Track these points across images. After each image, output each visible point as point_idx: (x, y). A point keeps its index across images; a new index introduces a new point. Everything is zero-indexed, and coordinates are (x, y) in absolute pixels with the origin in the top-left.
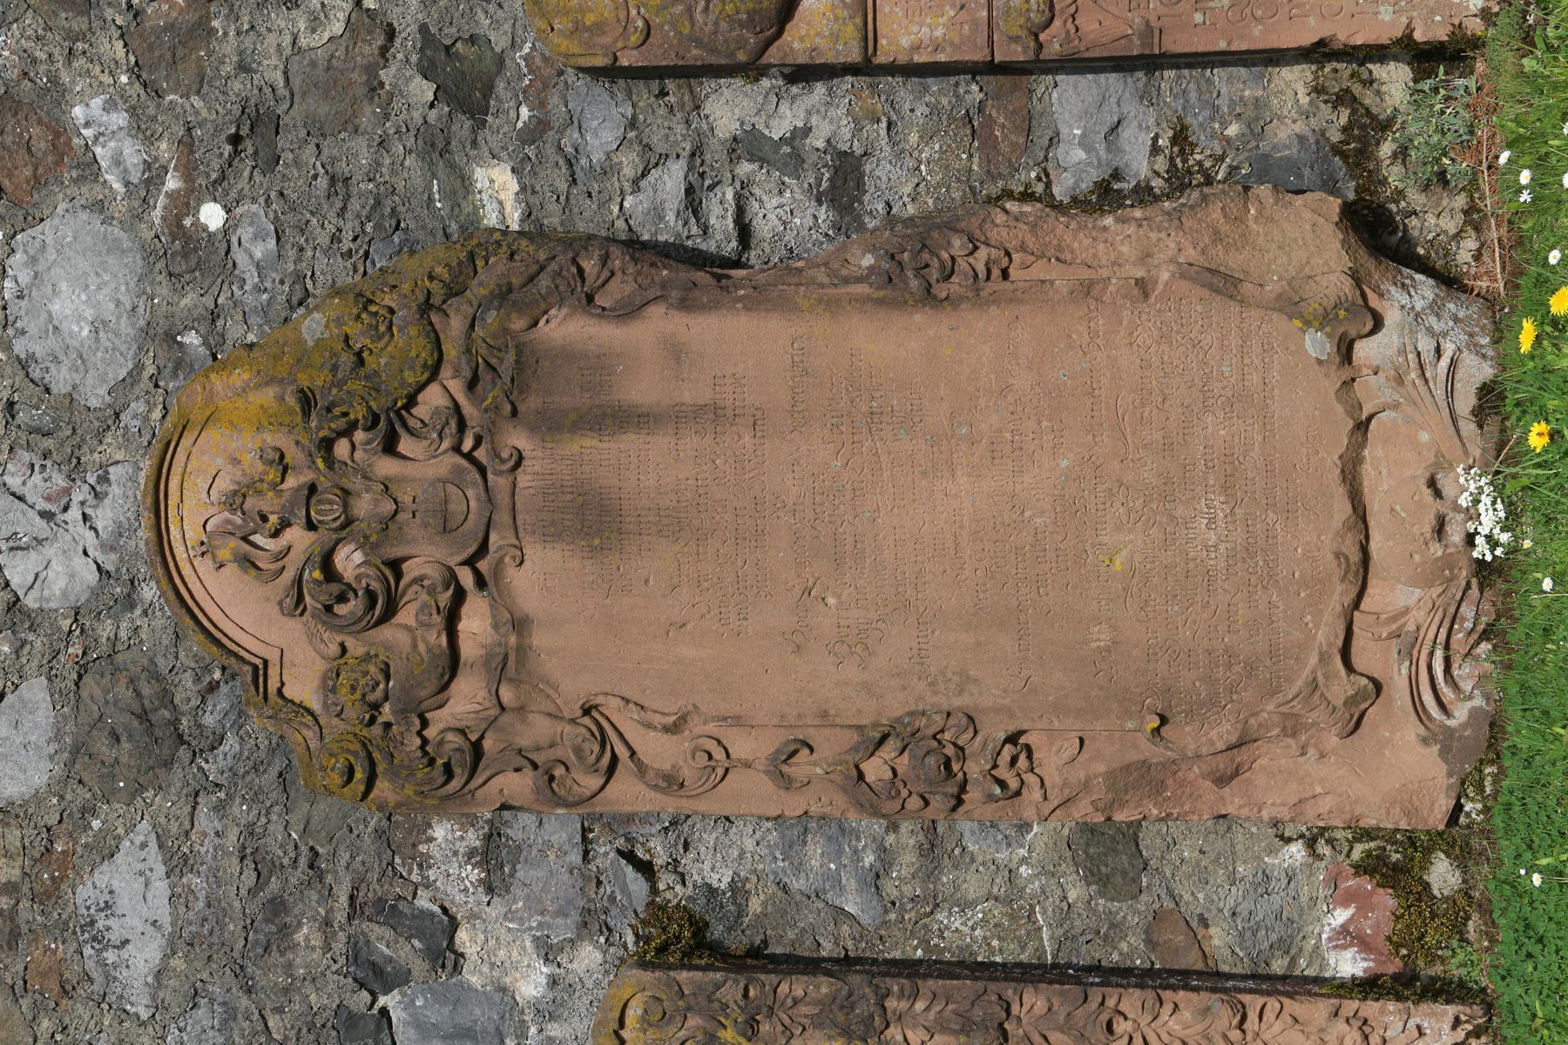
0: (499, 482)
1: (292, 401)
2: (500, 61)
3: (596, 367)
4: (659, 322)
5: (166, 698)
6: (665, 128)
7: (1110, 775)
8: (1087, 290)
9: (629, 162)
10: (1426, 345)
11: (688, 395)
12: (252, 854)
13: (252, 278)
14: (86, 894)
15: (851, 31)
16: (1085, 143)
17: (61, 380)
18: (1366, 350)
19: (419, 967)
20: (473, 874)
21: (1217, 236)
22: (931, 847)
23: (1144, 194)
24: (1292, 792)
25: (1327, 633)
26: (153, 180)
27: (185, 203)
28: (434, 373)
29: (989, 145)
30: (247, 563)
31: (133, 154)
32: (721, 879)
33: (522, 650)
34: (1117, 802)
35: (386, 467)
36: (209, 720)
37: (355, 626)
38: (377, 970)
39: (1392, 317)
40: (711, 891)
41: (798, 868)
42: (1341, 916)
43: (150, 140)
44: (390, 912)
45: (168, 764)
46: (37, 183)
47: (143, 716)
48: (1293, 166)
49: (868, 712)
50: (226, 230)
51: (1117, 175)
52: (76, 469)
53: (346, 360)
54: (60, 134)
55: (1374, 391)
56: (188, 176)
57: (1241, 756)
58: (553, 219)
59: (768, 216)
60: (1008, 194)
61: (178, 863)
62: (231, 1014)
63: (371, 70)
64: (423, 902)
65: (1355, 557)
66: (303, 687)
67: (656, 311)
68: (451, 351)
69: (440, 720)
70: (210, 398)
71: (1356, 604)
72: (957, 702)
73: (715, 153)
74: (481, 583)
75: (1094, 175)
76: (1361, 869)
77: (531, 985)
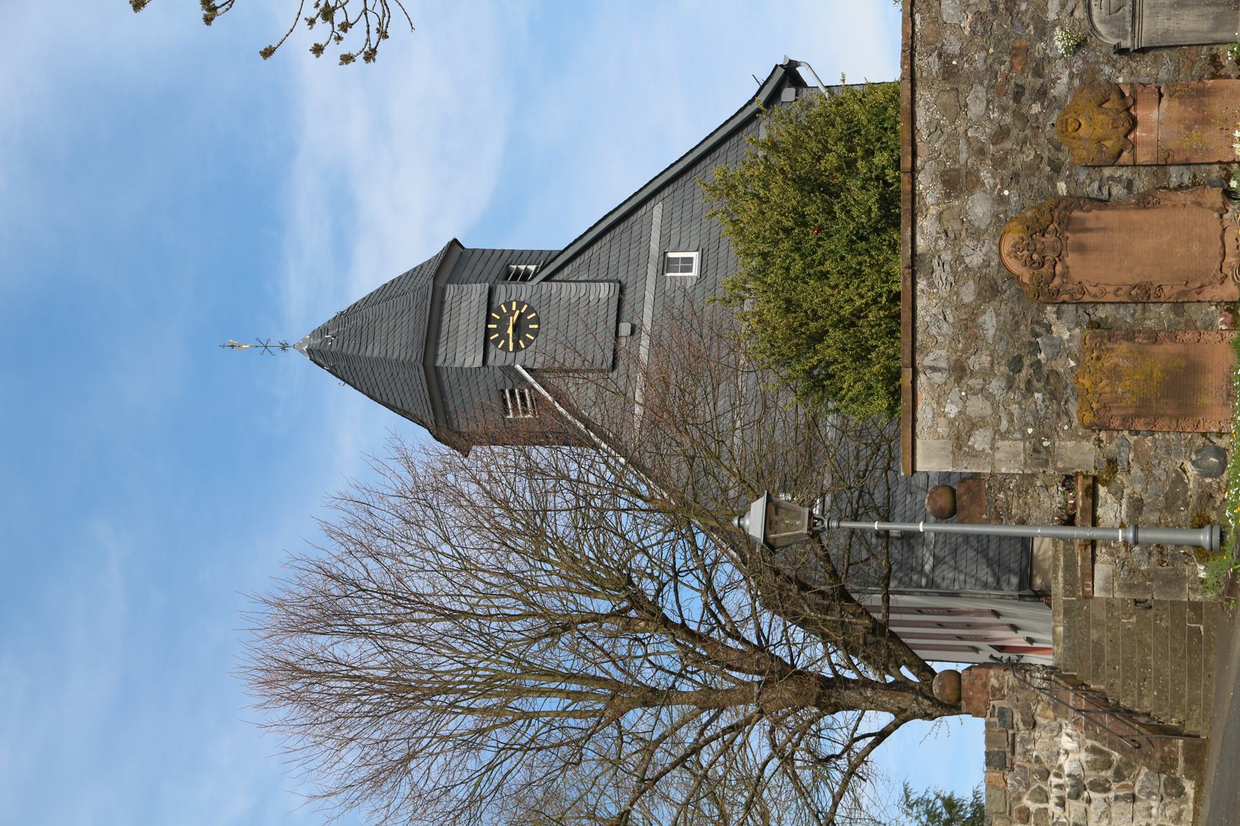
0: (1064, 242)
1: (1025, 227)
2: (1063, 163)
3: (1083, 221)
4: (1095, 212)
5: (996, 283)
6: (1095, 175)
7: (1177, 293)
8: (1174, 206)
9: (1088, 182)
10: (1236, 215)
11: (1099, 226)
12: (1012, 313)
13: (1014, 204)
14: (980, 320)
15: (1131, 159)
16: (1176, 177)
17: (976, 224)
18: (1225, 216)
19: (1044, 333)
20: (1055, 316)
21: (1199, 196)
22: (1144, 310)
23: (1187, 187)
24: (1211, 295)
25: (1217, 266)
26: (996, 187)
27: (1001, 190)
28: (1052, 222)
29: (1158, 178)
30: (1016, 257)
31: (992, 181)
32: (1103, 316)
33: (1068, 272)
34: (1178, 298)
35: (1043, 239)
36: (1004, 288)
37: (1035, 269)
38: (1036, 334)
39: (1230, 210)
40: (1101, 318)
41: (1118, 313)
42: (1222, 319)
43: (995, 179)
44: (1039, 323)
45: (996, 296)
46: (973, 187)
47: (992, 287)
48: (1215, 182)
49: (1132, 282)
50: (1009, 195)
51: (1182, 183)
52: (979, 240)
53: (1035, 220)
54: (978, 178)
55: (1226, 223)
56: (1002, 185)
57: (1202, 289)
58: (1073, 192)
59: (1115, 191)
60: (1161, 187)
61: (998, 315)
62: (1008, 343)
63: (1038, 165)
64: (1045, 321)
65: (1222, 252)
66: (1026, 280)
67: (1094, 211)
68: (1055, 218)
69: (1051, 285)
70: (1009, 228)
71: (1223, 261)
72: (1149, 280)
73: (1105, 180)
74: (1060, 260)
75: (1178, 183)
76: (1225, 310)
77: (1066, 336)
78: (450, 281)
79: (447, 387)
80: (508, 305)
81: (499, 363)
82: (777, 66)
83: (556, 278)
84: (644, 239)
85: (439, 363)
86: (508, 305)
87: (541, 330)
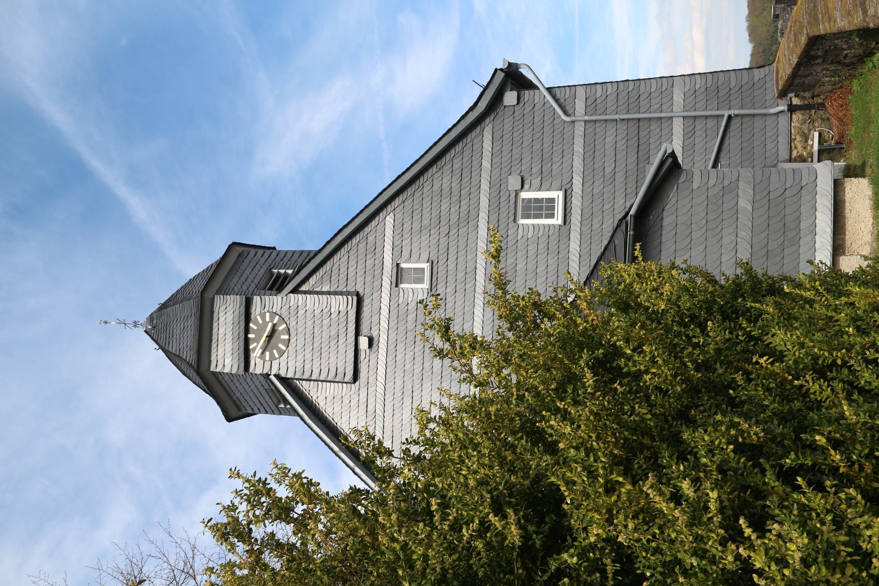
78: (219, 292)
79: (225, 385)
80: (263, 316)
81: (258, 371)
82: (496, 70)
83: (303, 288)
84: (376, 250)
85: (212, 369)
86: (263, 316)
87: (293, 341)
